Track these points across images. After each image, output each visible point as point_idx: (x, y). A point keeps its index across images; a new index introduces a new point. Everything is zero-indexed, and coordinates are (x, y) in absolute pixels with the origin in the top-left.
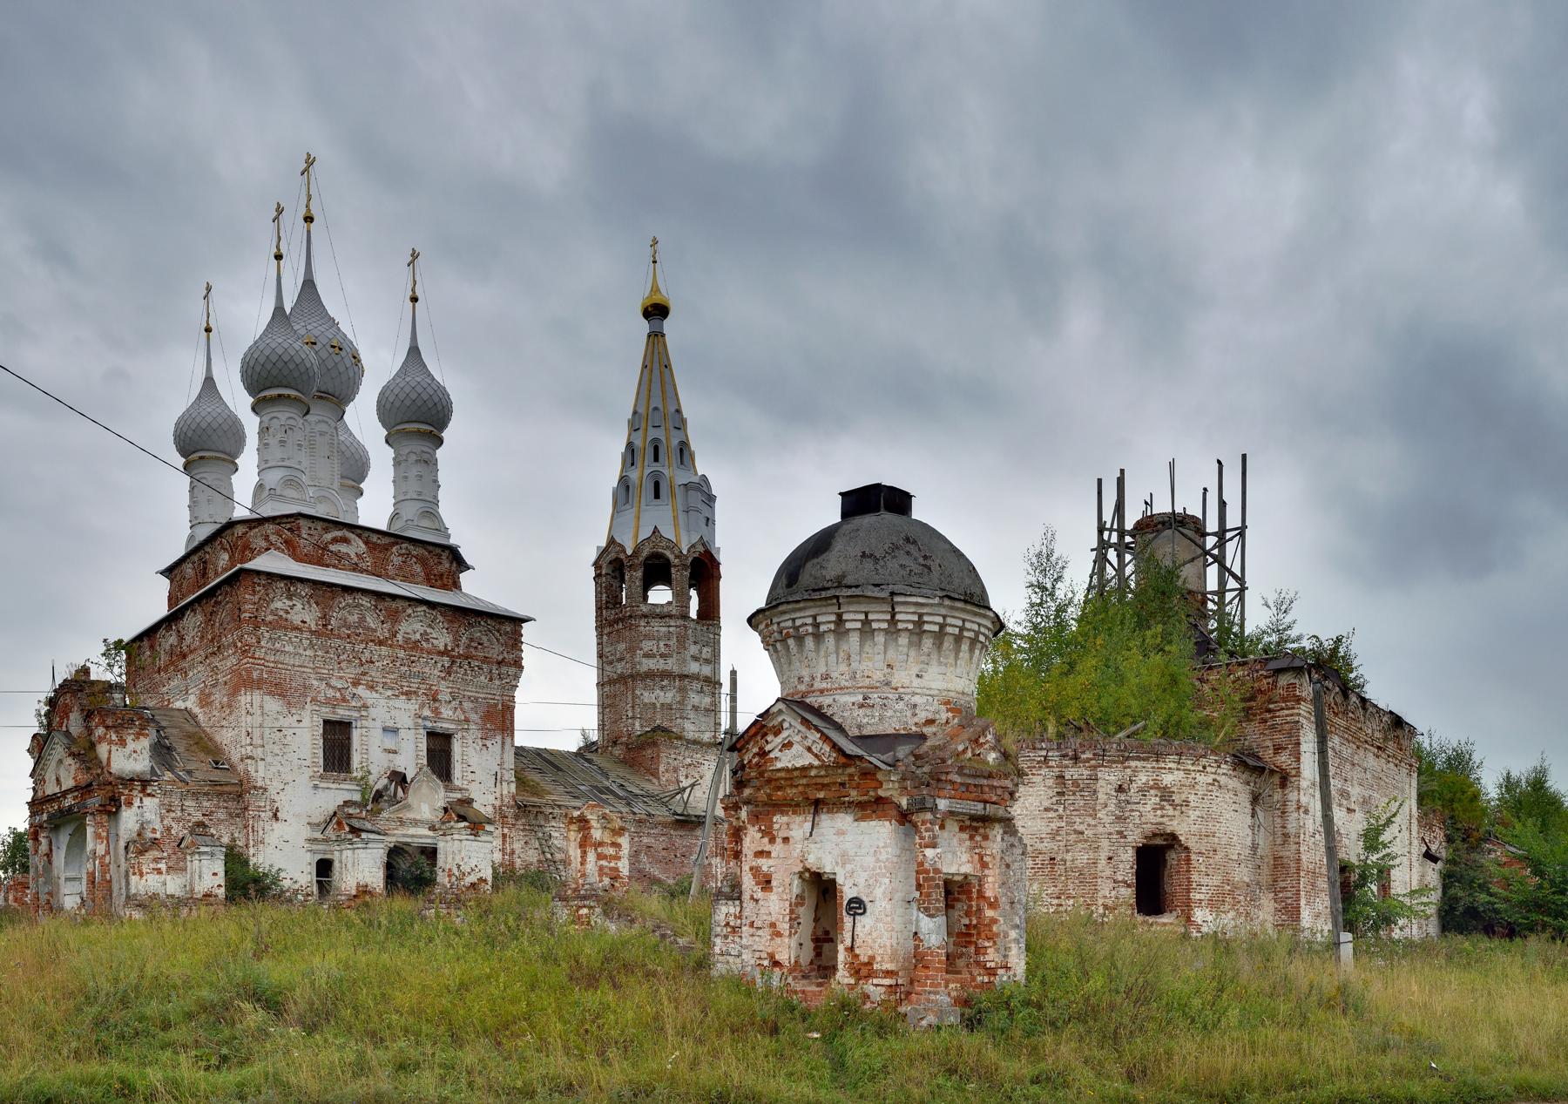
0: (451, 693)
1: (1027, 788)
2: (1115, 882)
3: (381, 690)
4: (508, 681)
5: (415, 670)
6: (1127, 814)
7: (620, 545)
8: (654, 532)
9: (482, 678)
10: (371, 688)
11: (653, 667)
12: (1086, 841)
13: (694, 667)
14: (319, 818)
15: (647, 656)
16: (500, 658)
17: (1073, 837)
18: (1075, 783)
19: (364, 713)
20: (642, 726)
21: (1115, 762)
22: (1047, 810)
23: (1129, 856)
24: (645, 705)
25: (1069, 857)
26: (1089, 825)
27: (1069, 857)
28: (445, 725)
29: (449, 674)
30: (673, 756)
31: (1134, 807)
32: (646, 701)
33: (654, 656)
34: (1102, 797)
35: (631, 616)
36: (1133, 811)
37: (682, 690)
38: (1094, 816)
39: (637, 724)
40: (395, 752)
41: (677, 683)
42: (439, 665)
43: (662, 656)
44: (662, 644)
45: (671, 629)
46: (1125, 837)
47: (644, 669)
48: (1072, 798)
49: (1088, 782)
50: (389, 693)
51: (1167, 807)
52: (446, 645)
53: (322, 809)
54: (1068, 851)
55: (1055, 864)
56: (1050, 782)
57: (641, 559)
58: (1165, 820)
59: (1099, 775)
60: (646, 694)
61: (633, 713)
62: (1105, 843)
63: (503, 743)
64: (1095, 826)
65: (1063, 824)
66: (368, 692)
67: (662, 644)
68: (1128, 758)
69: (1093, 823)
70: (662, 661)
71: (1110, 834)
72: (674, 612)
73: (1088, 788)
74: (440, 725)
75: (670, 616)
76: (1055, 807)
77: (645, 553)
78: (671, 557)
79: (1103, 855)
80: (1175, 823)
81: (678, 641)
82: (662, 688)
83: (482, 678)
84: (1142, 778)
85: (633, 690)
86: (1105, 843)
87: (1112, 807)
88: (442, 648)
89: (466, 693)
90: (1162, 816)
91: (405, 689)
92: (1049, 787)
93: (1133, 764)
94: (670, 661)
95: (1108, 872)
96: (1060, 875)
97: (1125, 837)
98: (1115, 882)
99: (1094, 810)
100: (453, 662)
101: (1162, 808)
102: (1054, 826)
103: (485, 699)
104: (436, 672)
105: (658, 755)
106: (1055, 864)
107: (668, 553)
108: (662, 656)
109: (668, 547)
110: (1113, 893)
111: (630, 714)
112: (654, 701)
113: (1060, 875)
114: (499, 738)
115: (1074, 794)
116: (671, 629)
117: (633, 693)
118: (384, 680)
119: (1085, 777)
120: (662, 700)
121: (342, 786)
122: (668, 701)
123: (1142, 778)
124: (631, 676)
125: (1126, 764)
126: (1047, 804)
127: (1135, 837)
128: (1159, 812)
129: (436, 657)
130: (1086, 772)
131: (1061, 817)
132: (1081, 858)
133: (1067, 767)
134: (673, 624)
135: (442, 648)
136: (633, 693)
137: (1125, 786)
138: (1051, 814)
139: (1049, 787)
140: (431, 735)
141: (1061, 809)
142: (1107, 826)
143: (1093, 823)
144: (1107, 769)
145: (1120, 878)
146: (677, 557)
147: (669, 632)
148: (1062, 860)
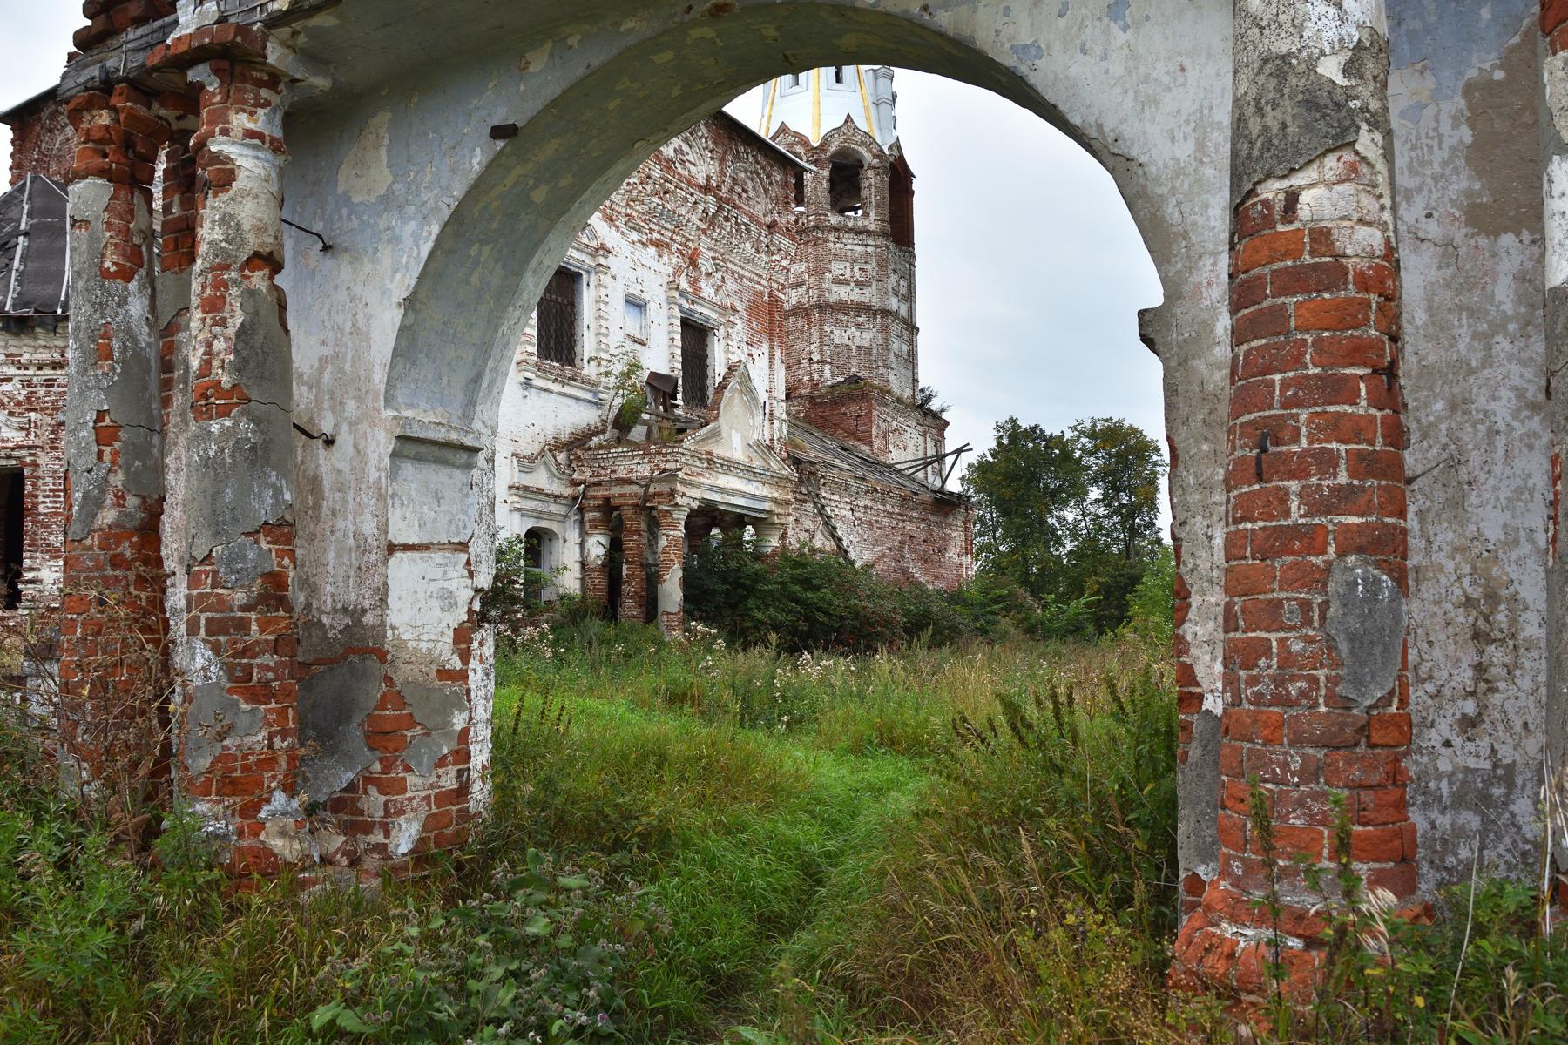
0: (714, 259)
3: (624, 228)
4: (778, 257)
5: (668, 206)
7: (797, 134)
8: (846, 122)
9: (748, 245)
10: (610, 219)
11: (845, 297)
13: (894, 304)
14: (529, 448)
15: (837, 281)
16: (768, 219)
19: (602, 261)
20: (833, 374)
24: (836, 346)
28: (706, 311)
29: (712, 224)
30: (883, 416)
32: (837, 341)
33: (847, 283)
35: (816, 227)
37: (884, 330)
39: (827, 371)
40: (642, 344)
41: (879, 320)
42: (700, 208)
43: (857, 283)
44: (856, 268)
45: (869, 249)
47: (833, 298)
50: (634, 236)
52: (708, 178)
53: (537, 429)
57: (828, 154)
60: (837, 332)
61: (822, 355)
63: (772, 356)
66: (605, 224)
67: (856, 268)
70: (857, 290)
72: (872, 227)
74: (698, 308)
75: (869, 233)
77: (833, 148)
78: (868, 156)
81: (878, 265)
82: (858, 326)
83: (748, 245)
85: (821, 326)
88: (702, 181)
89: (729, 265)
91: (656, 236)
94: (867, 291)
100: (720, 208)
103: (750, 280)
104: (694, 218)
105: (870, 412)
107: (863, 150)
108: (857, 283)
109: (863, 143)
111: (816, 357)
112: (847, 342)
114: (766, 346)
116: (869, 249)
117: (821, 329)
118: (629, 211)
120: (858, 341)
121: (567, 390)
122: (866, 343)
124: (819, 306)
129: (698, 195)
134: (871, 242)
135: (702, 181)
136: (821, 329)
140: (686, 323)
146: (875, 156)
147: (867, 253)
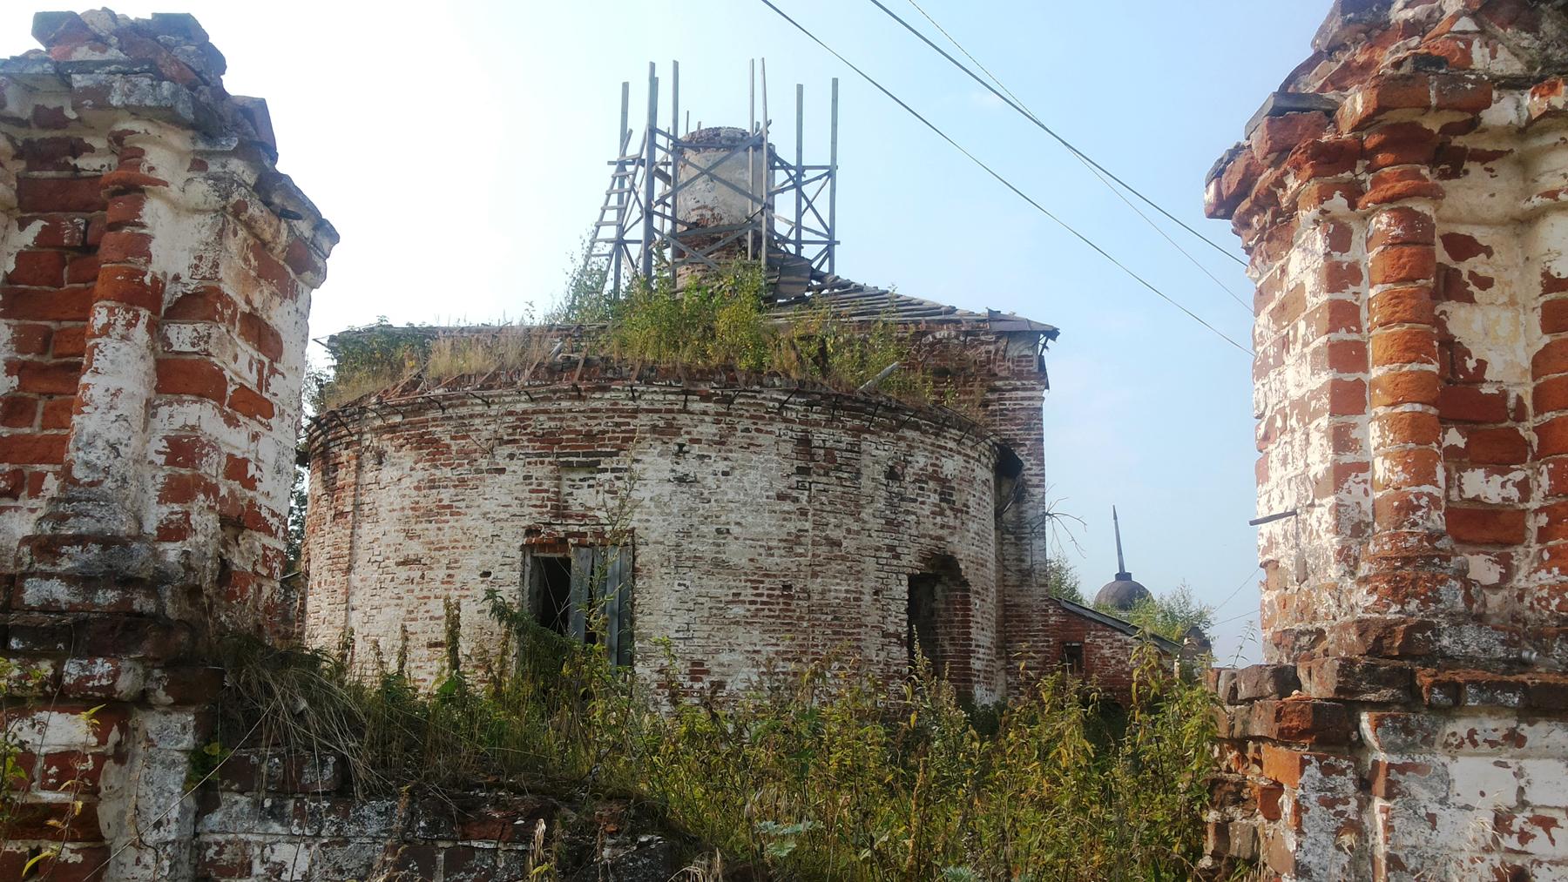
1: (747, 454)
2: (886, 635)
6: (901, 518)
12: (844, 558)
17: (823, 550)
18: (829, 452)
21: (884, 429)
22: (781, 497)
23: (901, 590)
25: (815, 585)
26: (849, 531)
27: (815, 585)
31: (910, 506)
34: (866, 484)
36: (908, 512)
38: (855, 515)
46: (897, 557)
48: (824, 479)
49: (848, 455)
51: (948, 512)
54: (815, 575)
55: (791, 597)
56: (787, 448)
58: (944, 532)
59: (864, 446)
62: (870, 564)
64: (858, 533)
65: (808, 525)
68: (903, 424)
69: (855, 527)
71: (878, 549)
73: (842, 464)
76: (795, 494)
79: (869, 586)
80: (956, 539)
84: (920, 460)
86: (870, 564)
87: (881, 505)
90: (942, 527)
92: (785, 457)
93: (909, 434)
95: (873, 619)
96: (801, 618)
97: (897, 557)
98: (886, 635)
99: (857, 505)
101: (942, 513)
102: (791, 527)
106: (791, 597)
110: (883, 655)
113: (801, 618)
115: (826, 474)
119: (843, 446)
123: (920, 460)
125: (900, 433)
126: (780, 486)
127: (910, 559)
128: (939, 519)
130: (847, 439)
131: (803, 513)
132: (839, 589)
133: (817, 424)
137: (898, 469)
138: (787, 506)
139: (785, 457)
141: (804, 497)
142: (874, 534)
143: (855, 527)
144: (874, 438)
145: (892, 629)
148: (804, 590)
